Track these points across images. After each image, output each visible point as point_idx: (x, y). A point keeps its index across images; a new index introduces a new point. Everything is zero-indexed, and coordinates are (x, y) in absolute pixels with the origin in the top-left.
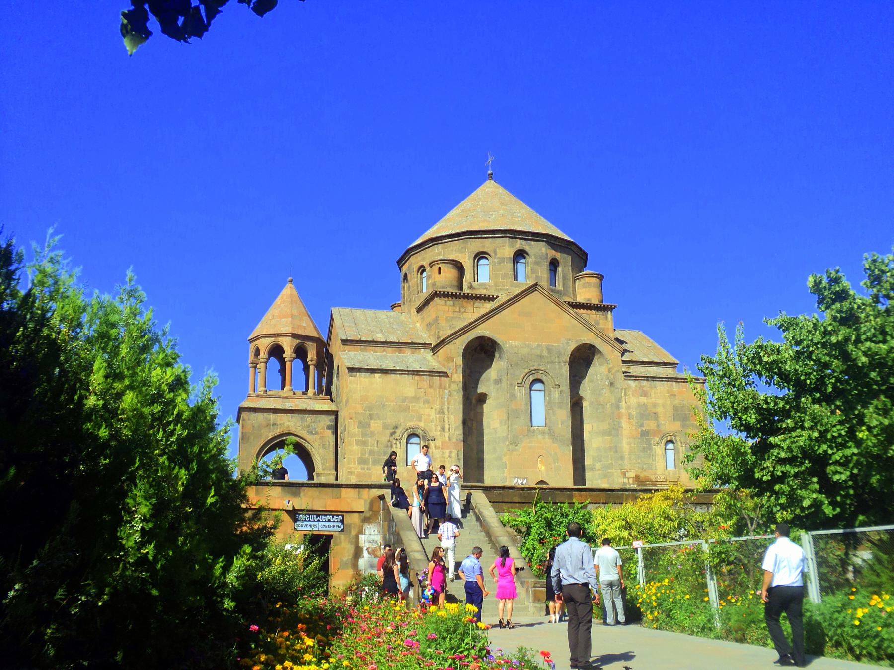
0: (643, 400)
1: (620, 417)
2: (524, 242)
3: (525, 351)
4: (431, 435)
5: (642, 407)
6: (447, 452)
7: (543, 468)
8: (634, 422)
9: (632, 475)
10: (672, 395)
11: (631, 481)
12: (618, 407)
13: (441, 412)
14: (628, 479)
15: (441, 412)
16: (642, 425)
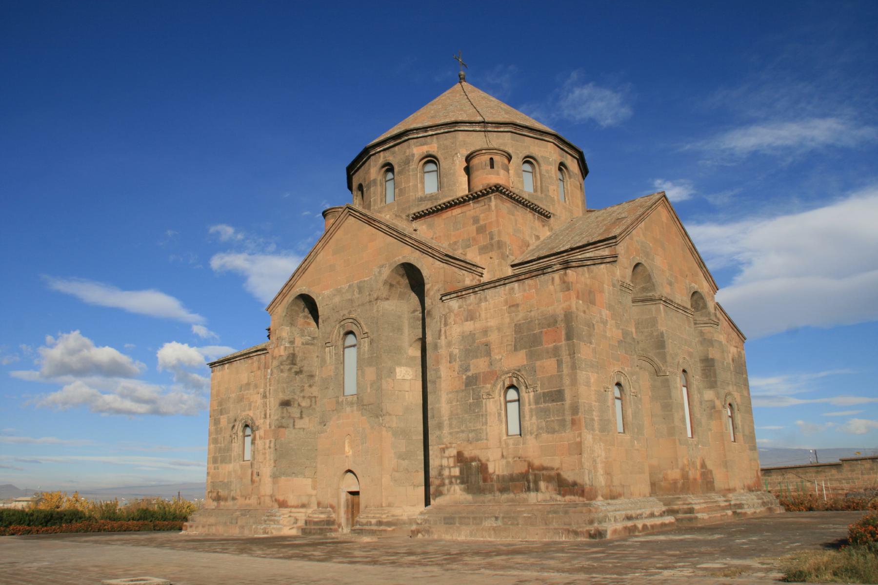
0: (469, 326)
1: (438, 362)
2: (387, 153)
3: (337, 300)
4: (257, 424)
5: (468, 338)
6: (267, 441)
7: (351, 453)
8: (456, 365)
9: (453, 452)
10: (514, 306)
11: (451, 461)
12: (436, 347)
13: (265, 397)
14: (448, 458)
15: (265, 397)
16: (467, 369)
